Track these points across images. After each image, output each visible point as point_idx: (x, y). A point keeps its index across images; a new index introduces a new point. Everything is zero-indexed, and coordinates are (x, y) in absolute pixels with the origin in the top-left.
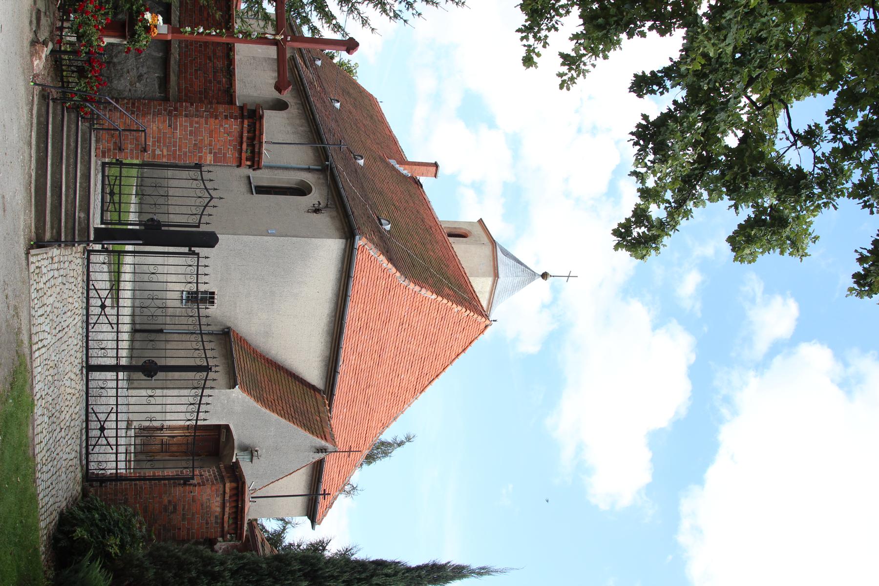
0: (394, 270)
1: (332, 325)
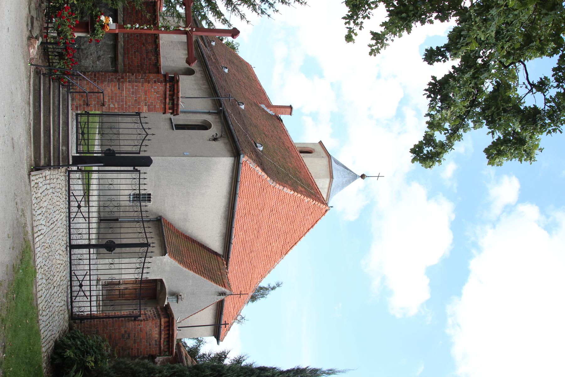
0: (266, 176)
1: (227, 213)
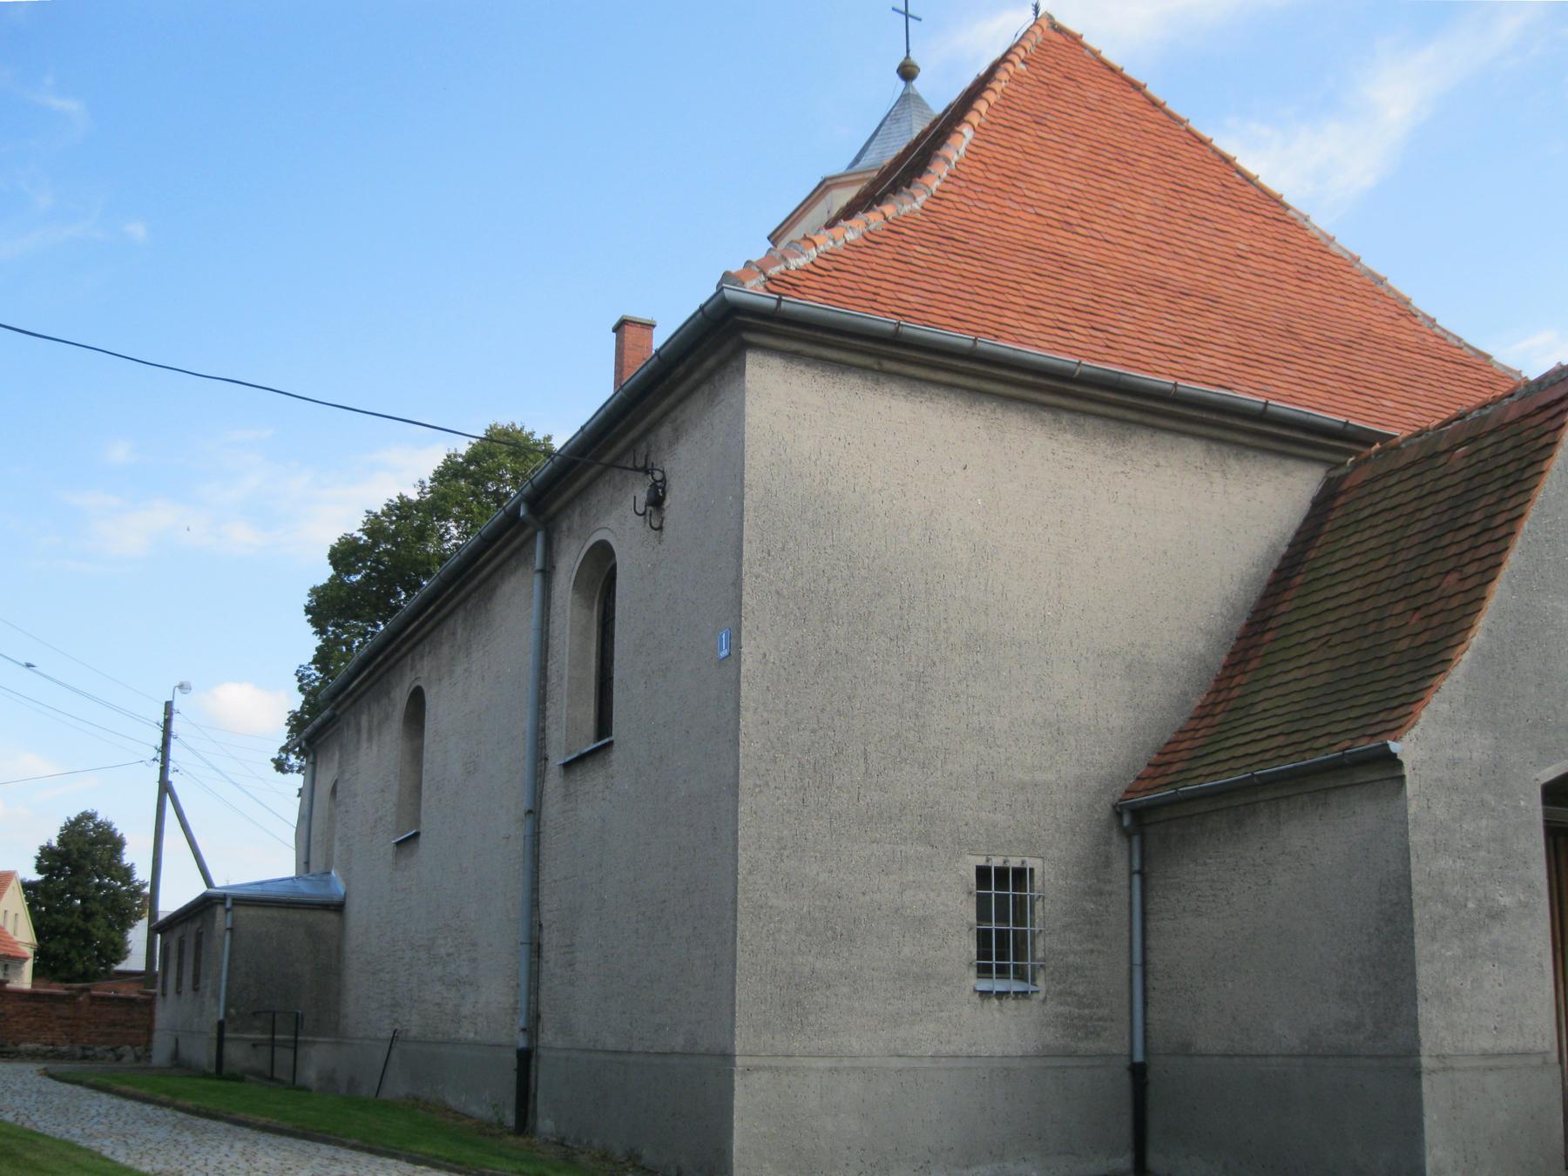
1: (1089, 424)
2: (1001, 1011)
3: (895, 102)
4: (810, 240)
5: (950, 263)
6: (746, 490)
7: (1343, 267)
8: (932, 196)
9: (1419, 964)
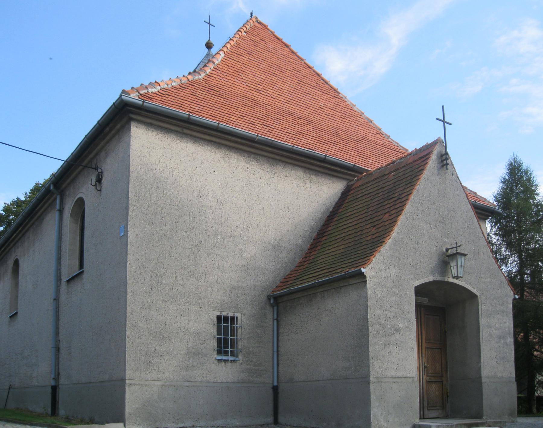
2: (225, 366)
3: (204, 56)
4: (158, 83)
5: (212, 98)
6: (130, 173)
7: (358, 116)
8: (207, 75)
9: (370, 346)
